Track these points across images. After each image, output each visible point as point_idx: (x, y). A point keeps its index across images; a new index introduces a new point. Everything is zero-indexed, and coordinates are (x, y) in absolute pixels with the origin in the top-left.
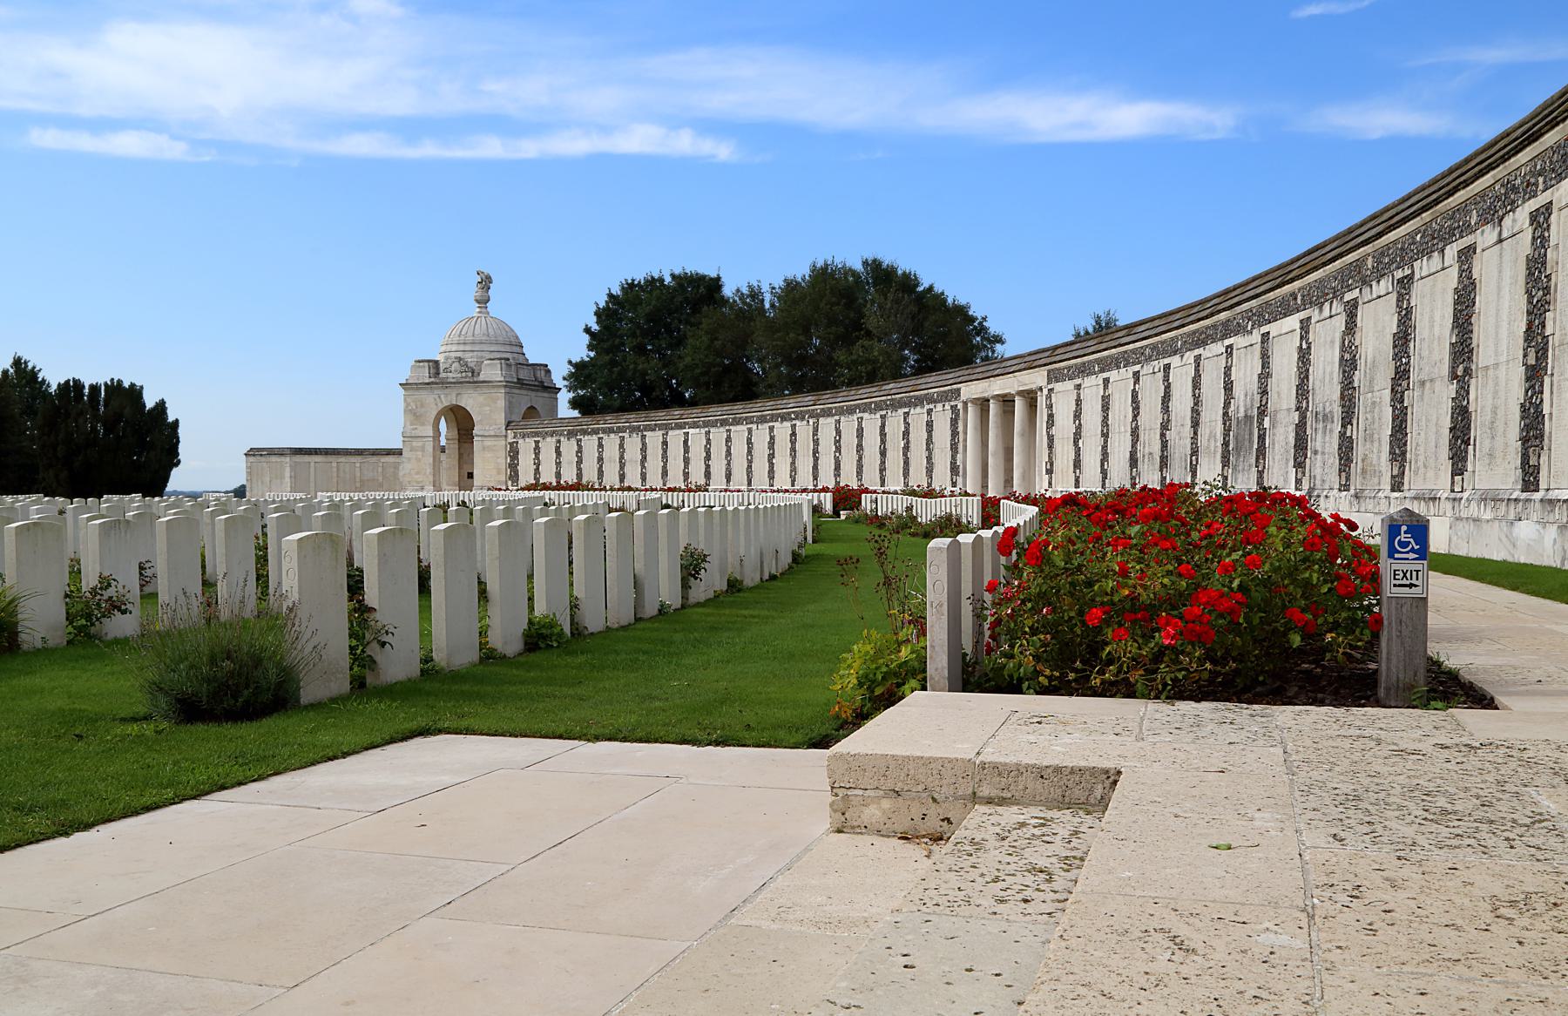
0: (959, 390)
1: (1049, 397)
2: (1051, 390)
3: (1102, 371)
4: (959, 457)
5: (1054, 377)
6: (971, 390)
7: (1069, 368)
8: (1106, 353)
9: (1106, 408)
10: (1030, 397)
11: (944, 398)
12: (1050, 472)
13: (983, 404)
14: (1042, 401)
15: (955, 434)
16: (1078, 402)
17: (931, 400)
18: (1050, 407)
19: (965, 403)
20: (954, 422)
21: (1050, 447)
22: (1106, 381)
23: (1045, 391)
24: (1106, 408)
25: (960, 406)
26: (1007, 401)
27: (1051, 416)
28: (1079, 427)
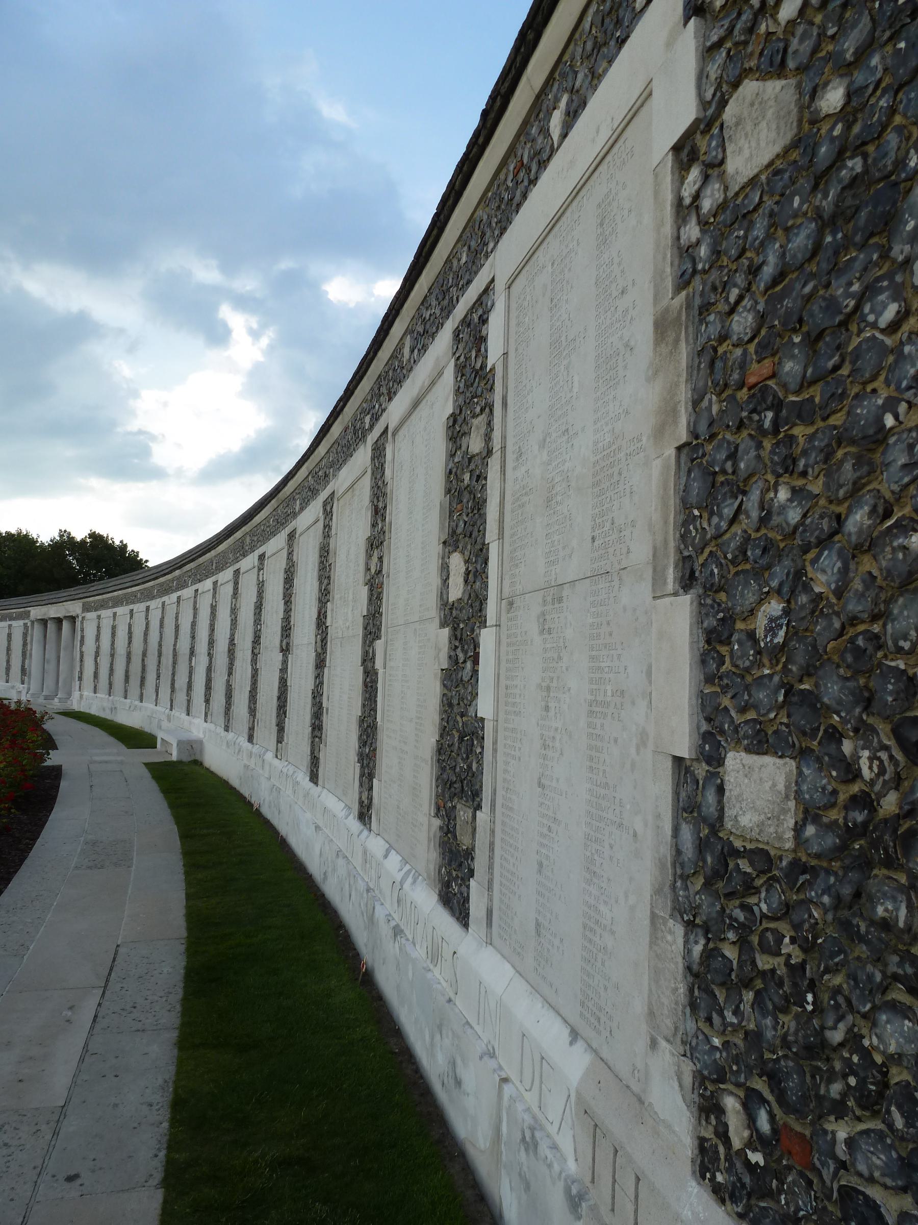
0: (29, 612)
1: (82, 623)
2: (83, 618)
3: (113, 607)
4: (27, 662)
5: (86, 608)
6: (36, 612)
7: (94, 602)
8: (115, 593)
9: (113, 634)
10: (72, 619)
11: (19, 617)
12: (80, 679)
13: (44, 622)
14: (78, 624)
15: (25, 644)
16: (99, 627)
17: (12, 619)
18: (82, 630)
19: (33, 622)
20: (25, 635)
21: (81, 661)
22: (115, 614)
23: (80, 618)
24: (113, 634)
25: (29, 624)
26: (59, 621)
27: (83, 637)
28: (98, 648)
